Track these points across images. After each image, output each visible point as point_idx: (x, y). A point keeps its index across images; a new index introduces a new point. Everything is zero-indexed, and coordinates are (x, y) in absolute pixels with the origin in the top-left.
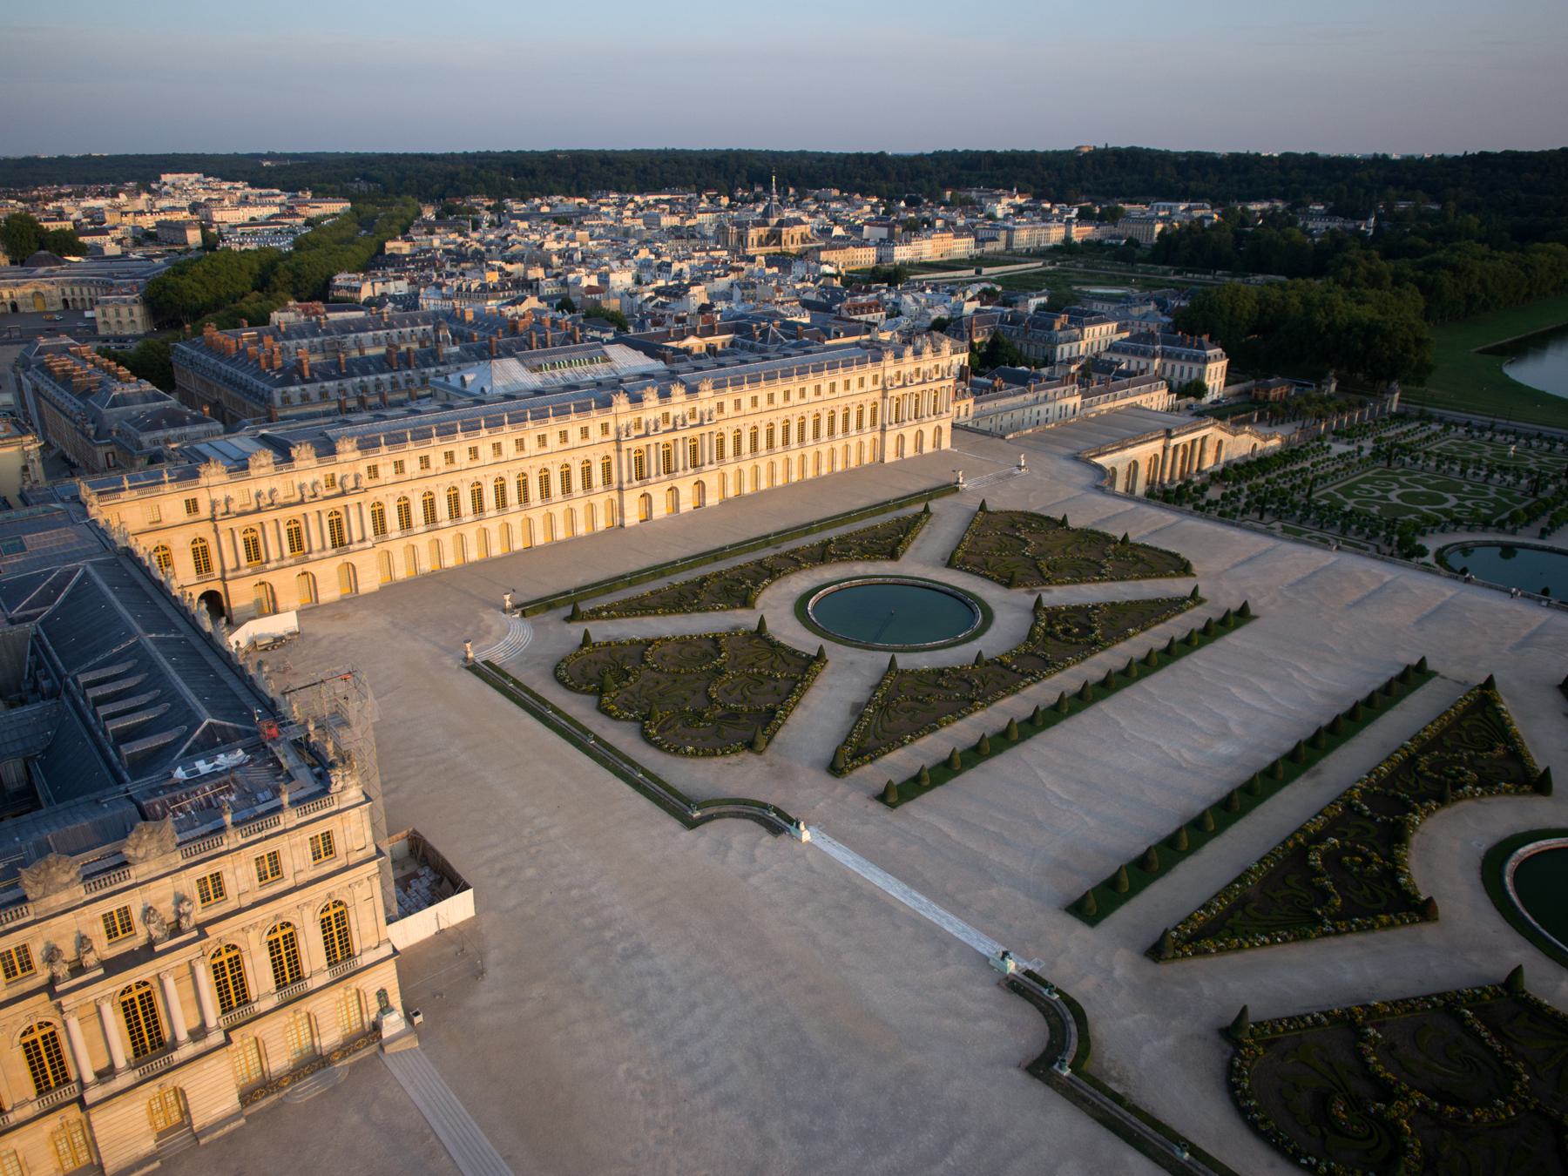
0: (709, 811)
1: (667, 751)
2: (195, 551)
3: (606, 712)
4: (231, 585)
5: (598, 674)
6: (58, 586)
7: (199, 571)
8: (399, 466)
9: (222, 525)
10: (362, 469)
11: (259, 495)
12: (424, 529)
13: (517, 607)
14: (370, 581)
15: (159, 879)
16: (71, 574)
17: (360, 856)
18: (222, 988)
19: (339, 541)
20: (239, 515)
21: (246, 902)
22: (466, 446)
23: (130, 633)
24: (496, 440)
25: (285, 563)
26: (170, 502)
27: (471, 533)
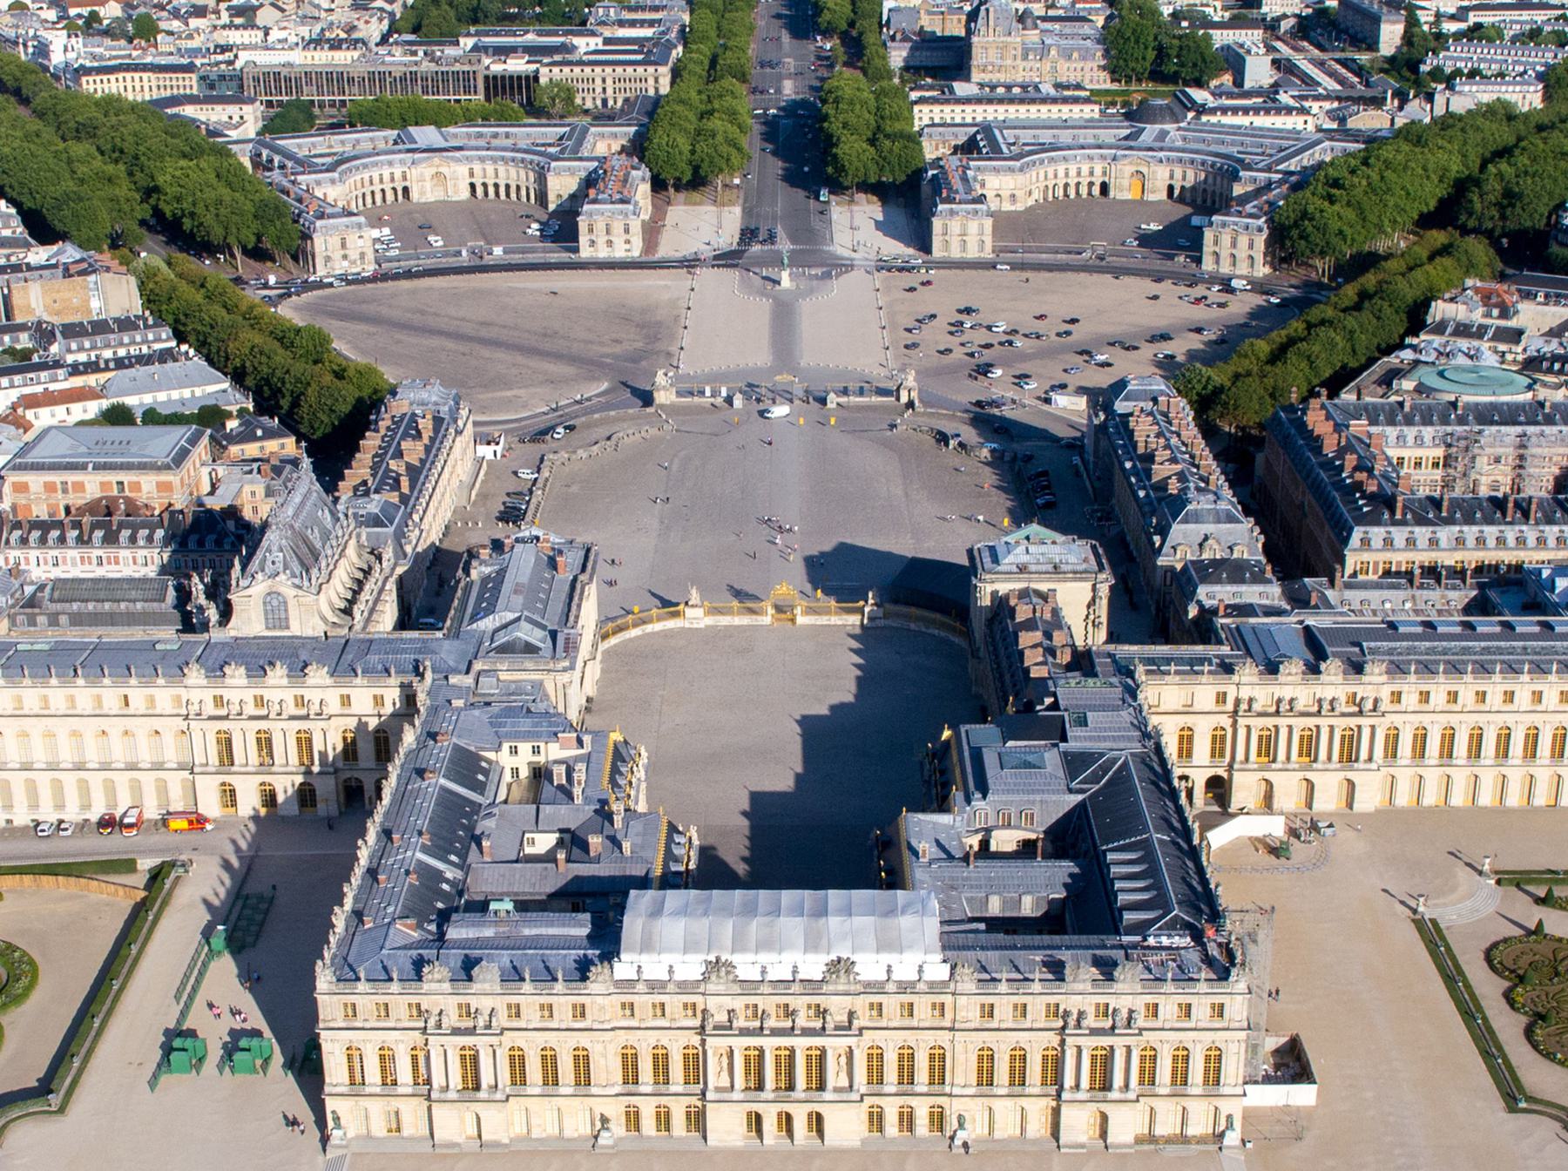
0: (1535, 1107)
1: (1540, 1052)
2: (1214, 737)
3: (1511, 1002)
4: (1236, 775)
5: (1527, 966)
6: (1105, 769)
7: (1213, 755)
8: (1425, 697)
9: (1242, 722)
10: (1385, 693)
11: (1279, 701)
12: (1435, 762)
13: (1496, 872)
14: (1369, 798)
15: (1128, 993)
16: (1115, 760)
17: (1237, 1025)
18: (1142, 1071)
19: (1349, 756)
20: (1260, 715)
21: (1167, 1026)
22: (1501, 688)
23: (1146, 830)
24: (1538, 688)
25: (1290, 766)
26: (1205, 692)
27: (1488, 778)
